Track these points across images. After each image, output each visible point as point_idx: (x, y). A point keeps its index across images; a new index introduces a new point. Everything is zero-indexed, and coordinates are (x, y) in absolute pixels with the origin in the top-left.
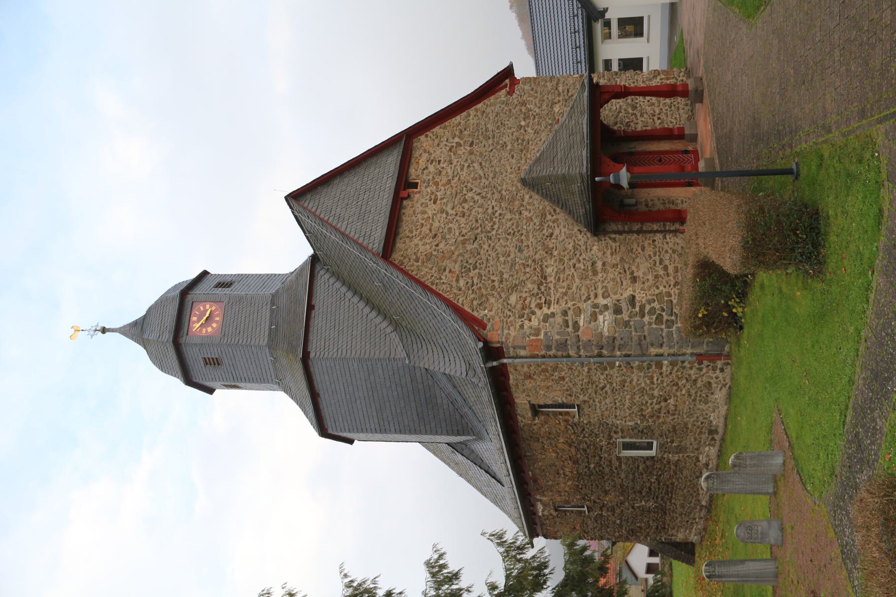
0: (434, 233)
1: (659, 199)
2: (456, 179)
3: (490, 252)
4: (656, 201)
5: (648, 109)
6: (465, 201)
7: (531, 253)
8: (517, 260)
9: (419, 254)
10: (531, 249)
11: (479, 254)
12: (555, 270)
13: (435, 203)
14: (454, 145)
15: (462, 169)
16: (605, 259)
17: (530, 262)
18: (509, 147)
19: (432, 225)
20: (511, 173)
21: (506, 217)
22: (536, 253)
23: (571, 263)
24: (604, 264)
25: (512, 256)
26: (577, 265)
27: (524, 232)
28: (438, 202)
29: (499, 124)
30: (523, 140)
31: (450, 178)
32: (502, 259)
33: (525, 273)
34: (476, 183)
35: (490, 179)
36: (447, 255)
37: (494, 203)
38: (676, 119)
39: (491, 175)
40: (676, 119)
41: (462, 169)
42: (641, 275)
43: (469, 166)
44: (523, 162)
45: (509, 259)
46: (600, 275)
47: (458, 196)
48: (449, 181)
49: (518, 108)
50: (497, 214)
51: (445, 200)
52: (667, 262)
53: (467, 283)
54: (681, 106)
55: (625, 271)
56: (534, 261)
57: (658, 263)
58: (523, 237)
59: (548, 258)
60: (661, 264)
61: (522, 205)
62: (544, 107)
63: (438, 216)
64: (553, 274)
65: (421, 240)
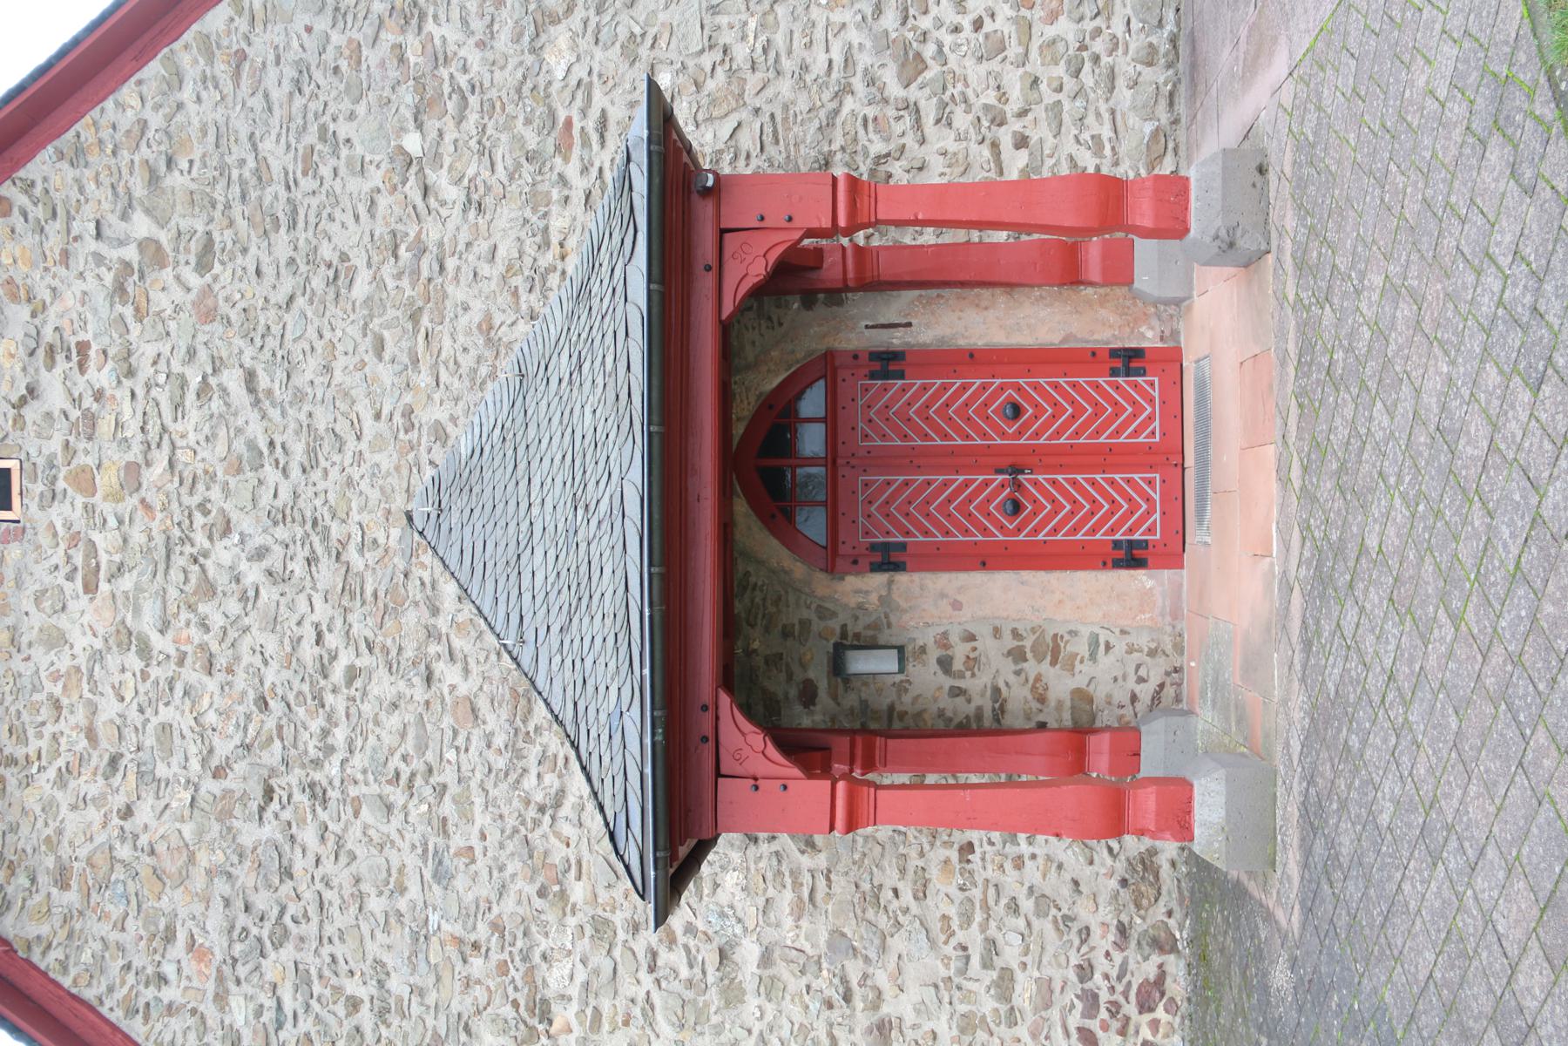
0: (107, 745)
1: (997, 632)
2: (161, 459)
3: (328, 866)
4: (988, 645)
5: (976, 72)
6: (208, 589)
7: (485, 890)
8: (434, 919)
9: (65, 851)
10: (481, 864)
11: (287, 873)
12: (581, 976)
13: (90, 588)
14: (131, 253)
15: (178, 406)
16: (771, 935)
17: (483, 931)
18: (361, 289)
19: (93, 710)
20: (378, 445)
21: (375, 690)
22: (502, 890)
23: (640, 946)
24: (766, 960)
25: (414, 891)
26: (665, 957)
27: (448, 776)
28: (104, 587)
29: (311, 137)
30: (420, 250)
31: (135, 453)
32: (376, 904)
33: (468, 983)
34: (243, 486)
35: (295, 472)
36: (171, 866)
37: (322, 612)
38: (1097, 144)
39: (298, 449)
40: (1096, 138)
41: (178, 406)
42: (910, 1017)
43: (204, 390)
44: (424, 379)
45: (402, 904)
46: (752, 1003)
47: (179, 561)
48: (133, 472)
49: (389, 37)
50: (338, 673)
51: (127, 583)
52: (1011, 954)
53: (259, 1012)
54: (1126, 66)
55: (847, 998)
56: (497, 927)
57: (975, 961)
58: (448, 808)
59: (551, 917)
60: (987, 964)
61: (432, 634)
62: (503, 40)
63: (113, 661)
64: (574, 991)
65: (61, 781)
